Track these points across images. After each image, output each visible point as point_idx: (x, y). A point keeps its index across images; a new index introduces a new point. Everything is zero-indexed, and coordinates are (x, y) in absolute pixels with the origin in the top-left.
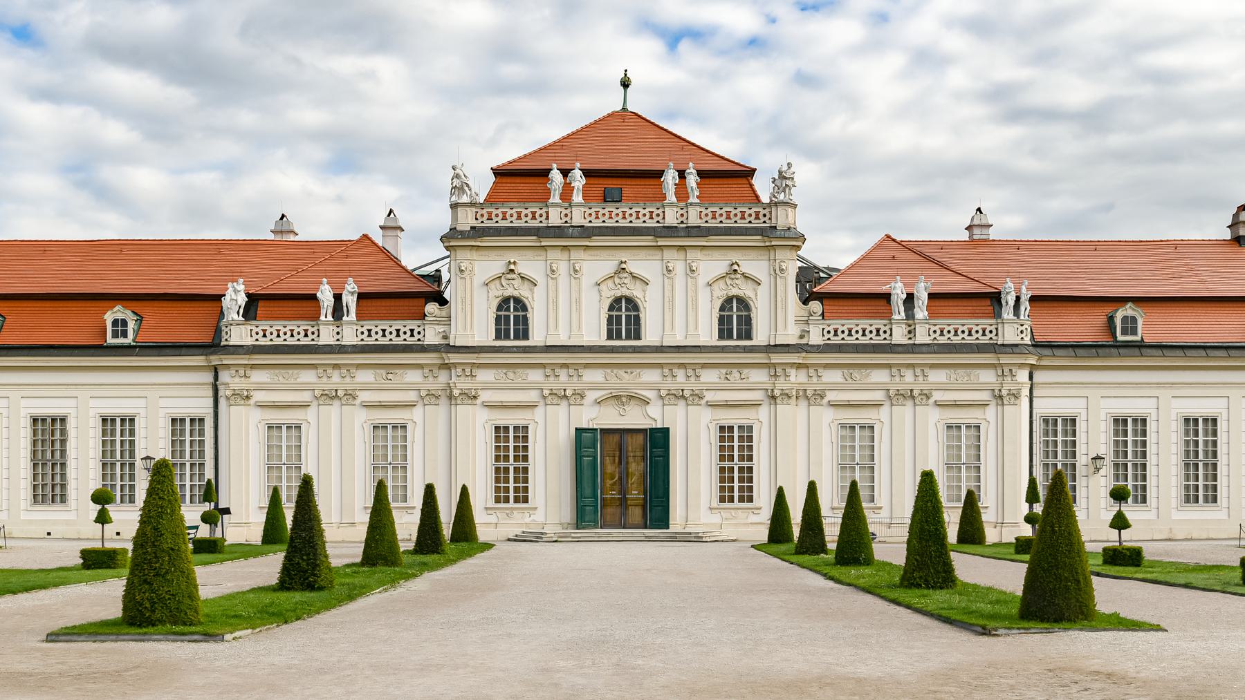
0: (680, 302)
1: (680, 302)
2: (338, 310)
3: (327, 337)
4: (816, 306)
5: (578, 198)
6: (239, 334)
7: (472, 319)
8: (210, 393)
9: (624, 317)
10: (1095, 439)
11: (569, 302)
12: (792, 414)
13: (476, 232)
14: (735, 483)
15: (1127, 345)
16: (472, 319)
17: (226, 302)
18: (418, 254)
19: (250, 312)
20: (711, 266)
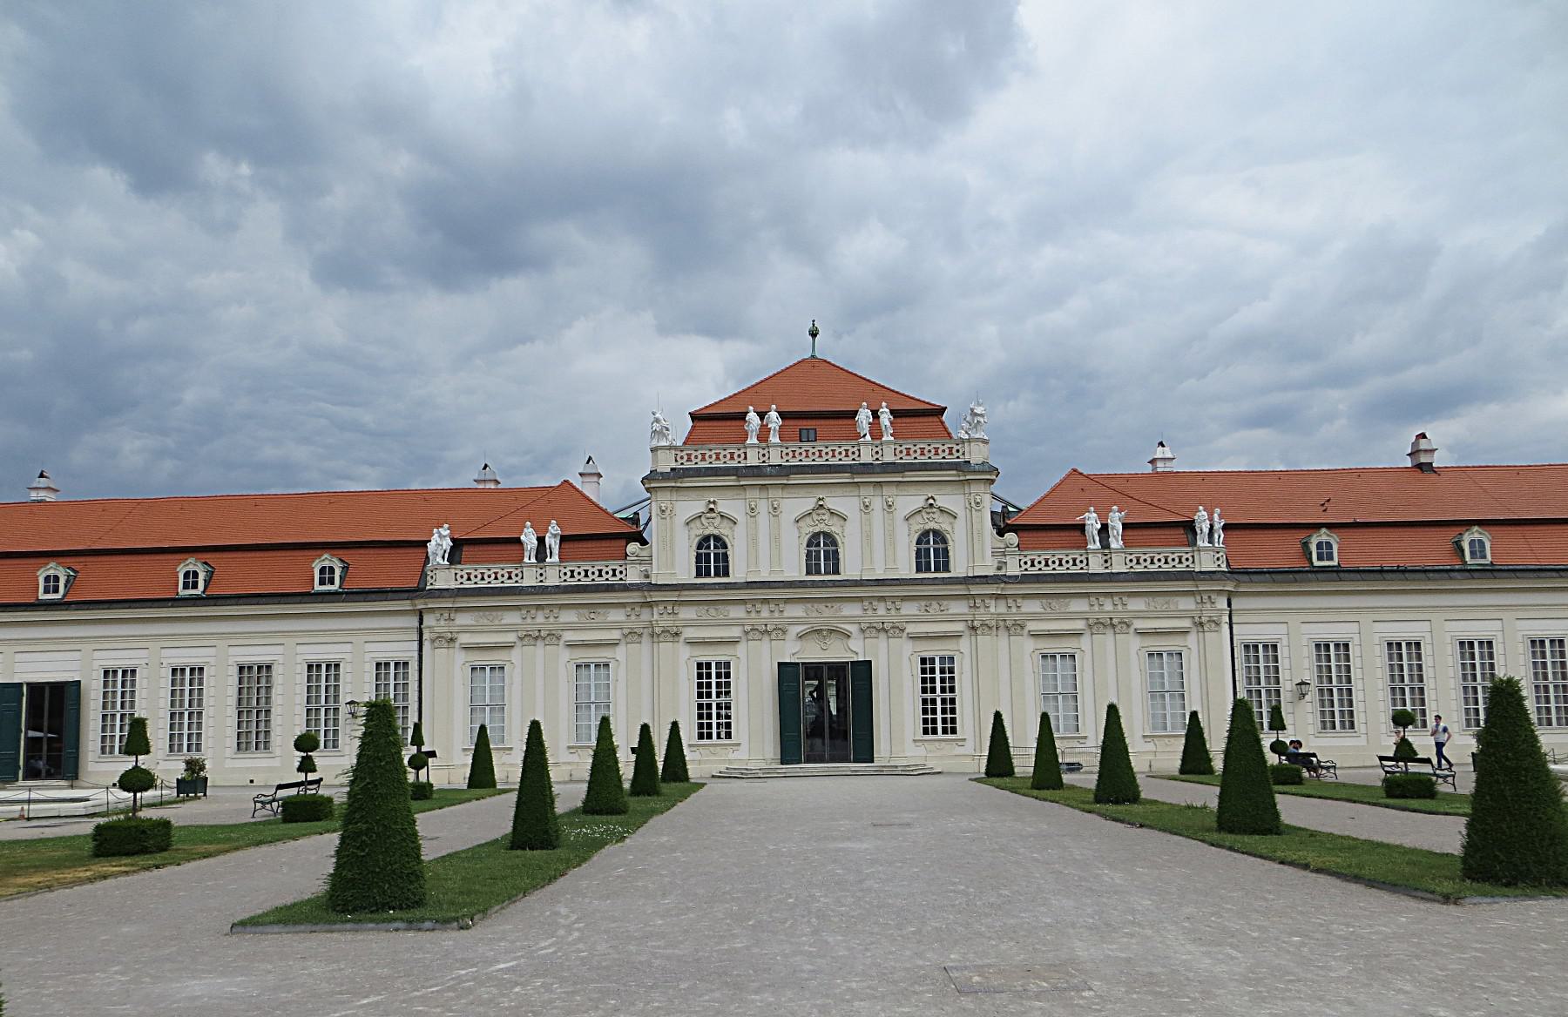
0: (877, 538)
1: (877, 538)
2: (541, 551)
3: (530, 580)
4: (1011, 537)
5: (774, 439)
6: (443, 579)
7: (671, 556)
8: (416, 637)
9: (823, 550)
10: (1297, 665)
11: (767, 540)
12: (995, 646)
13: (676, 473)
14: (938, 716)
15: (1323, 570)
16: (671, 556)
17: (431, 547)
18: (615, 491)
19: (454, 557)
20: (909, 501)
